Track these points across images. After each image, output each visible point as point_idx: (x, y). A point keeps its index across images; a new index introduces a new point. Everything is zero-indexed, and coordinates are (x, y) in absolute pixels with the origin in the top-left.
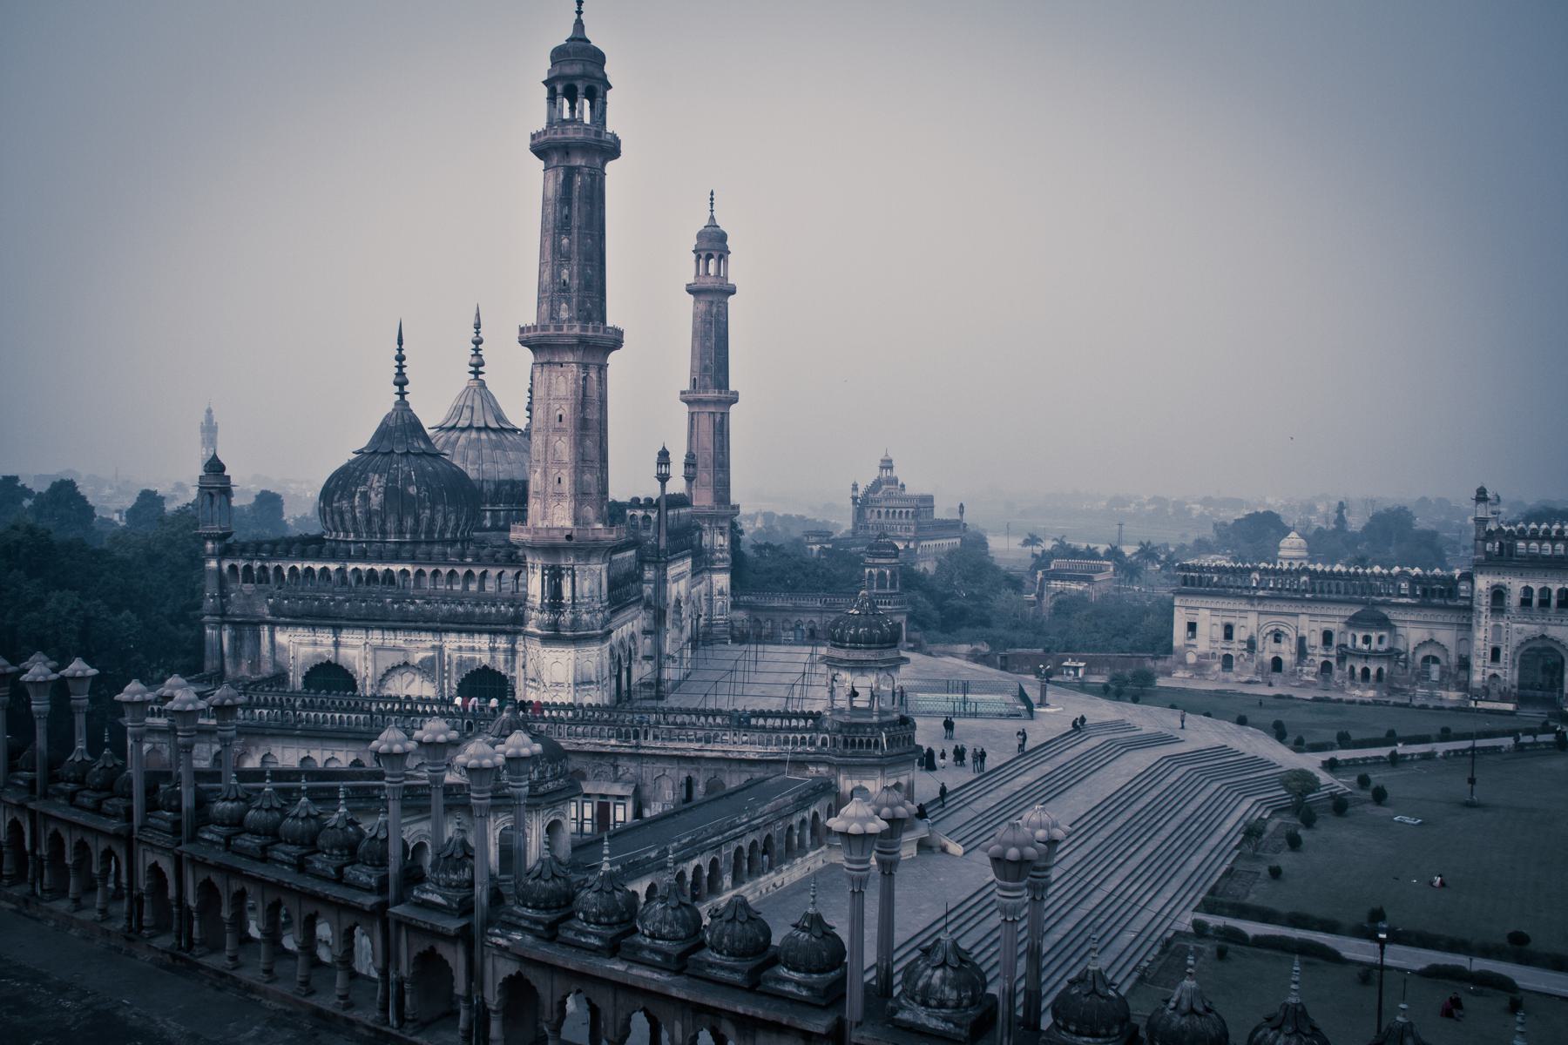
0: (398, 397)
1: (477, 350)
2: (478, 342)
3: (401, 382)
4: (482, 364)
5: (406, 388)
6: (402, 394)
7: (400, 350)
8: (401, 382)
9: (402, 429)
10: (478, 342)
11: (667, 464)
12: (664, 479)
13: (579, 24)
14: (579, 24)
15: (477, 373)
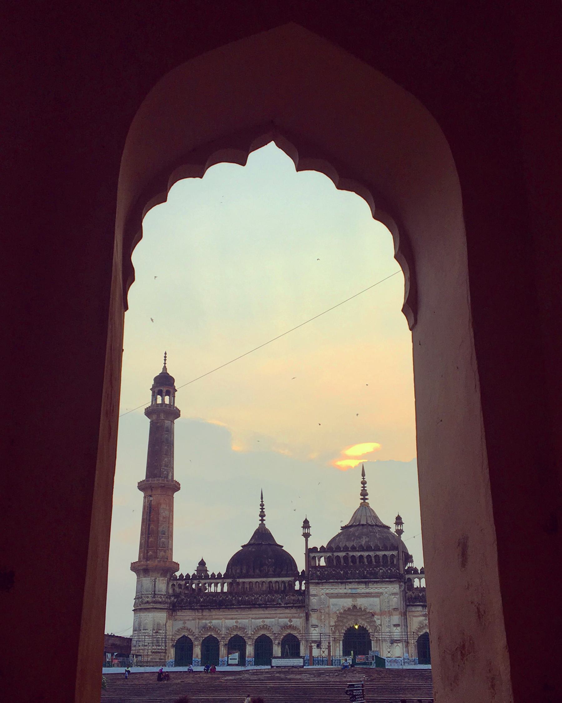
0: (260, 522)
1: (364, 487)
2: (364, 483)
3: (262, 515)
4: (367, 495)
5: (264, 518)
6: (262, 520)
7: (262, 501)
8: (262, 515)
9: (262, 536)
10: (364, 483)
11: (309, 527)
12: (307, 536)
13: (165, 368)
14: (165, 368)
15: (364, 499)
